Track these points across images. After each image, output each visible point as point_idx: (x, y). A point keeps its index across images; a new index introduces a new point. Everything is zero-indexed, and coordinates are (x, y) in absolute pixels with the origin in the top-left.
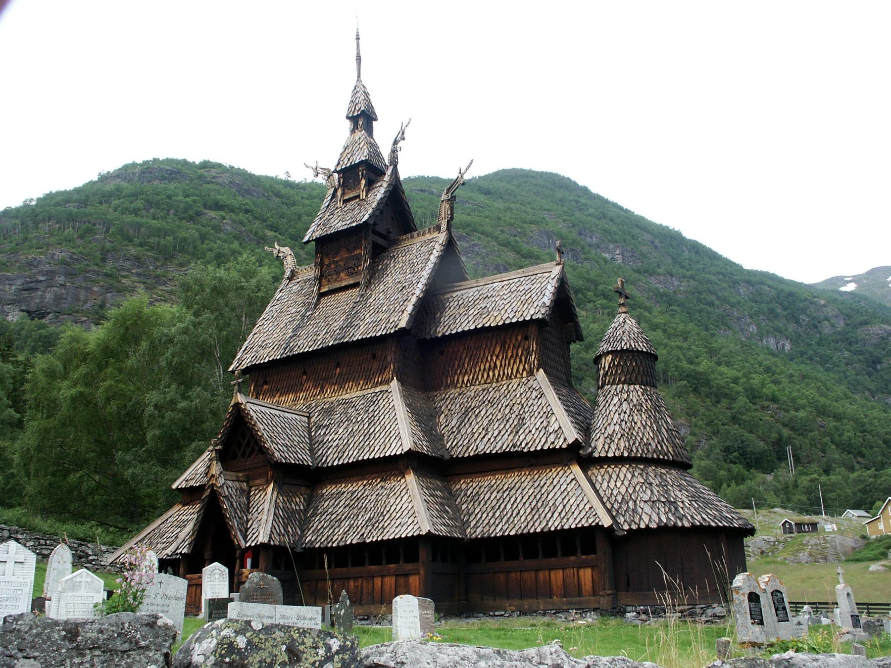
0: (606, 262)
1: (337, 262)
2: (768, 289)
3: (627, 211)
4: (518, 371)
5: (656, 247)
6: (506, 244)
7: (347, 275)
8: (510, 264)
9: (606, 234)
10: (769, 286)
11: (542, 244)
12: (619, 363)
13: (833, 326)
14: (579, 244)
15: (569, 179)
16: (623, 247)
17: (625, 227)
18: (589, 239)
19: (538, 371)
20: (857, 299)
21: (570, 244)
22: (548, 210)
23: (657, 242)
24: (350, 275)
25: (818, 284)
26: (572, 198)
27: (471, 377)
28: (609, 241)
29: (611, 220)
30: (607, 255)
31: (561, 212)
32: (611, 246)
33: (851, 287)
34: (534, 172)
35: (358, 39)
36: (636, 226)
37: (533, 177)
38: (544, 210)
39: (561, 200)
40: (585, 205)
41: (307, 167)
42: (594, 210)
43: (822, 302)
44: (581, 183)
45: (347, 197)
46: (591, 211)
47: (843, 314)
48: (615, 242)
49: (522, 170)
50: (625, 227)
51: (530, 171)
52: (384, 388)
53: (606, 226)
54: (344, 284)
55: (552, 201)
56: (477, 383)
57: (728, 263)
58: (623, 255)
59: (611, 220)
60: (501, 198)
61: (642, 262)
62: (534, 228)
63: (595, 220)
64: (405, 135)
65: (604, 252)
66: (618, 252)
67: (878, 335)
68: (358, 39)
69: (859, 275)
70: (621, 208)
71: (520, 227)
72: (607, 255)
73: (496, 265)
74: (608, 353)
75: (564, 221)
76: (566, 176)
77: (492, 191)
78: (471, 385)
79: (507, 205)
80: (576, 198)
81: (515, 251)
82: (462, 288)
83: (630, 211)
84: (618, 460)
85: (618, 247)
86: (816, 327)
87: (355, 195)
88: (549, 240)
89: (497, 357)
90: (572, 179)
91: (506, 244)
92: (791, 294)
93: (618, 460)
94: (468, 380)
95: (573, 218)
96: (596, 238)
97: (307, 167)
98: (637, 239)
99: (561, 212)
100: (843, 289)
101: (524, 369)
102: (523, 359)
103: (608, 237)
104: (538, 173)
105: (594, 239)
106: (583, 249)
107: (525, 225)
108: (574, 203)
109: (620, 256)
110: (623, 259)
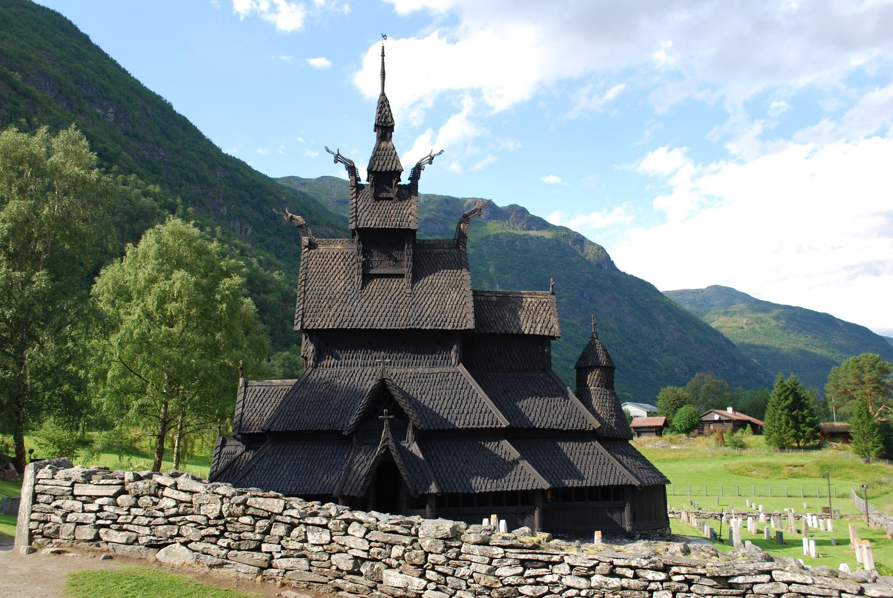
0: (99, 118)
2: (240, 176)
5: (147, 114)
10: (242, 174)
15: (70, 22)
17: (122, 88)
23: (149, 109)
25: (277, 179)
29: (109, 77)
30: (99, 111)
32: (105, 103)
35: (383, 56)
36: (132, 89)
41: (328, 151)
43: (284, 198)
44: (83, 29)
46: (90, 62)
50: (122, 88)
53: (104, 82)
57: (209, 143)
58: (115, 114)
59: (109, 77)
61: (132, 126)
63: (93, 73)
65: (98, 107)
66: (111, 110)
68: (383, 56)
69: (311, 179)
70: (118, 66)
72: (99, 111)
75: (62, 65)
80: (76, 45)
83: (127, 72)
88: (46, 82)
92: (260, 186)
96: (92, 91)
97: (328, 151)
98: (132, 102)
103: (104, 94)
105: (89, 92)
108: (73, 50)
109: (113, 115)
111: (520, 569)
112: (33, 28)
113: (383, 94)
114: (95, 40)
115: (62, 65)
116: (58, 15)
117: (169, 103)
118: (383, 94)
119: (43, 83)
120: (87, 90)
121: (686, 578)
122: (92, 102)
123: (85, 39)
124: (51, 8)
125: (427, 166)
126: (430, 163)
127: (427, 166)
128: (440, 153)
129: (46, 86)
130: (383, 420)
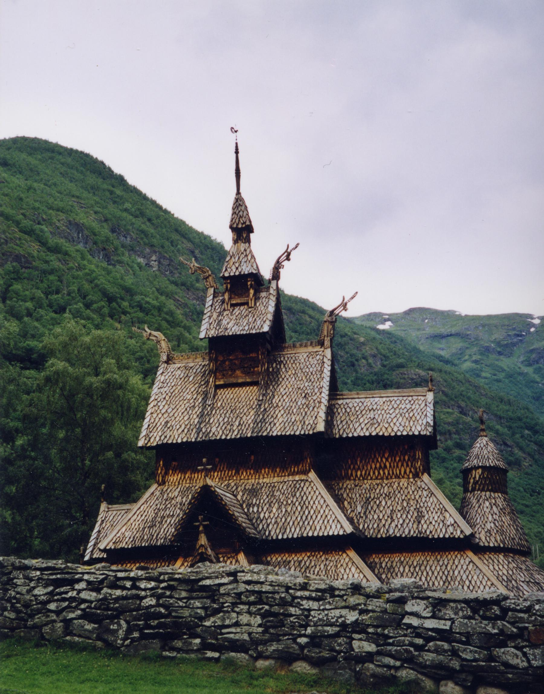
0: (140, 268)
1: (231, 360)
2: (308, 319)
3: (166, 212)
4: (405, 472)
6: (29, 232)
7: (242, 372)
8: (33, 257)
9: (143, 236)
10: (310, 316)
11: (70, 238)
12: (487, 475)
13: (370, 365)
14: (112, 243)
15: (102, 163)
16: (160, 253)
17: (164, 230)
18: (122, 238)
19: (422, 474)
20: (394, 339)
21: (102, 242)
22: (78, 197)
23: (197, 252)
24: (247, 373)
25: (356, 318)
26: (105, 186)
27: (363, 472)
28: (145, 244)
29: (149, 220)
31: (93, 202)
33: (387, 326)
34: (62, 147)
35: (237, 152)
36: (176, 230)
37: (60, 154)
38: (73, 196)
39: (92, 188)
40: (121, 198)
42: (130, 205)
43: (362, 339)
44: (117, 170)
45: (234, 302)
46: (127, 205)
47: (381, 354)
48: (152, 246)
49: (46, 142)
50: (164, 230)
51: (57, 145)
52: (303, 477)
53: (143, 226)
54: (240, 381)
55: (82, 187)
56: (369, 478)
60: (20, 173)
61: (180, 274)
62: (62, 216)
63: (131, 217)
64: (291, 257)
65: (139, 256)
66: (154, 258)
67: (412, 379)
68: (237, 152)
69: (397, 314)
70: (160, 207)
71: (45, 213)
72: (141, 260)
73: (16, 256)
74: (479, 467)
75: (96, 213)
76: (100, 158)
77: (10, 162)
78: (364, 479)
79: (29, 183)
80: (110, 188)
81: (40, 242)
82: (345, 397)
83: (170, 212)
84: (496, 550)
85: (155, 252)
86: (353, 365)
87: (243, 301)
88: (78, 233)
89: (387, 460)
90: (108, 163)
91: (29, 232)
93: (496, 550)
94: (361, 475)
95: (106, 211)
98: (177, 246)
99: (93, 202)
100: (381, 327)
101: (411, 471)
102: (410, 464)
103: (145, 240)
104: (66, 149)
105: (128, 239)
106: (116, 249)
107: (51, 211)
108: (107, 194)
109: (157, 263)
110: (159, 267)
111: (51, 588)
112: (61, 173)
113: (238, 193)
114: (131, 180)
115: (96, 213)
116: (87, 155)
117: (219, 244)
118: (238, 193)
119: (76, 235)
120: (126, 237)
121: (168, 584)
122: (133, 250)
123: (121, 180)
124: (80, 149)
125: (286, 263)
126: (288, 259)
127: (286, 263)
128: (296, 247)
129: (79, 238)
130: (198, 527)
